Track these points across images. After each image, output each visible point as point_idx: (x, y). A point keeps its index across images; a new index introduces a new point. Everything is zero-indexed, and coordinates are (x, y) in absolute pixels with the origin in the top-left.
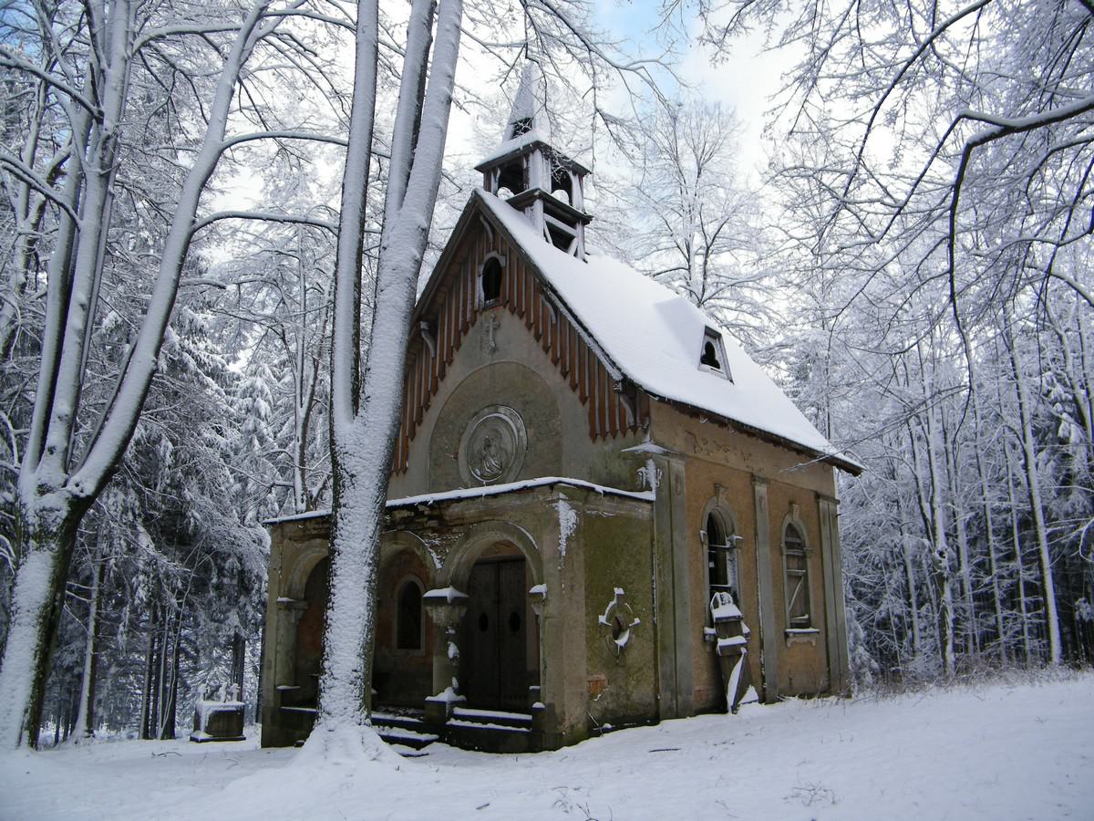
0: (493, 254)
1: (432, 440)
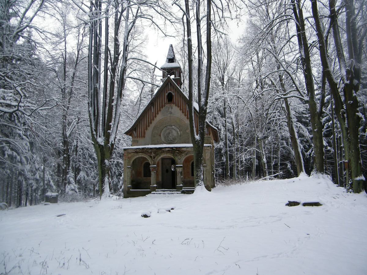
1: (153, 131)
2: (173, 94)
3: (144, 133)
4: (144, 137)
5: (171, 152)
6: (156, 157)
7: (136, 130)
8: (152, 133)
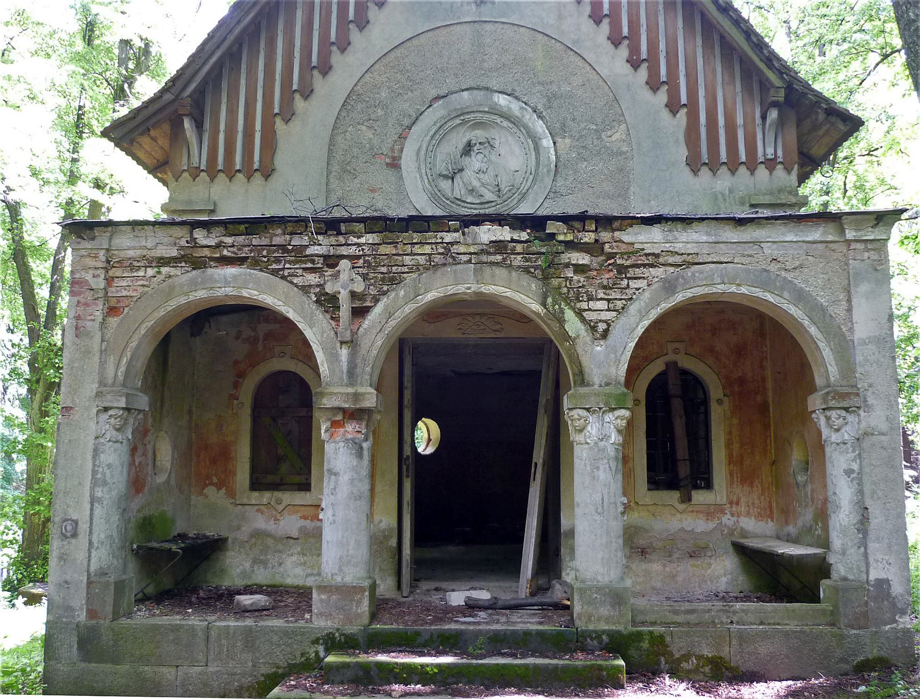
3: (270, 143)
4: (267, 172)
5: (518, 260)
6: (379, 309)
7: (207, 125)
8: (332, 143)
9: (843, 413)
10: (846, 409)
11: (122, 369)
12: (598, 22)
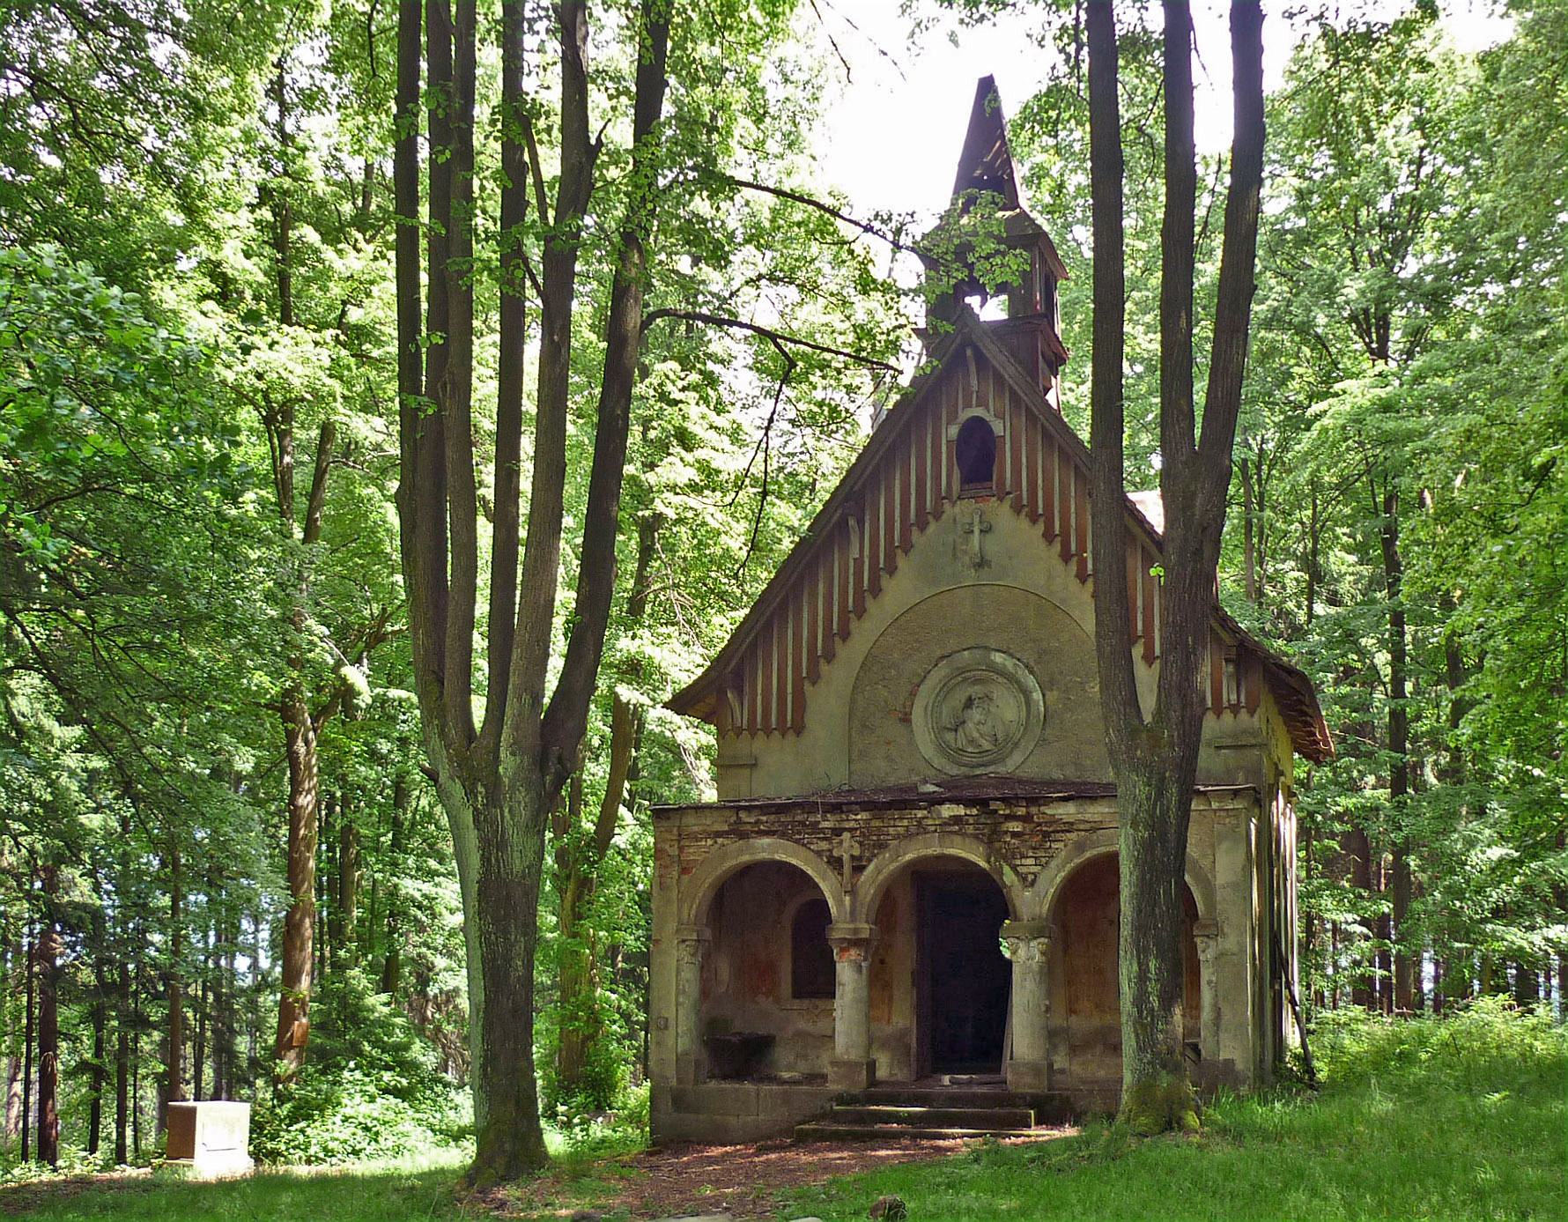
0: (978, 412)
2: (998, 427)
4: (799, 729)
5: (970, 830)
6: (871, 867)
7: (747, 689)
8: (853, 701)
9: (1206, 939)
10: (1208, 937)
11: (693, 912)
12: (1083, 582)
